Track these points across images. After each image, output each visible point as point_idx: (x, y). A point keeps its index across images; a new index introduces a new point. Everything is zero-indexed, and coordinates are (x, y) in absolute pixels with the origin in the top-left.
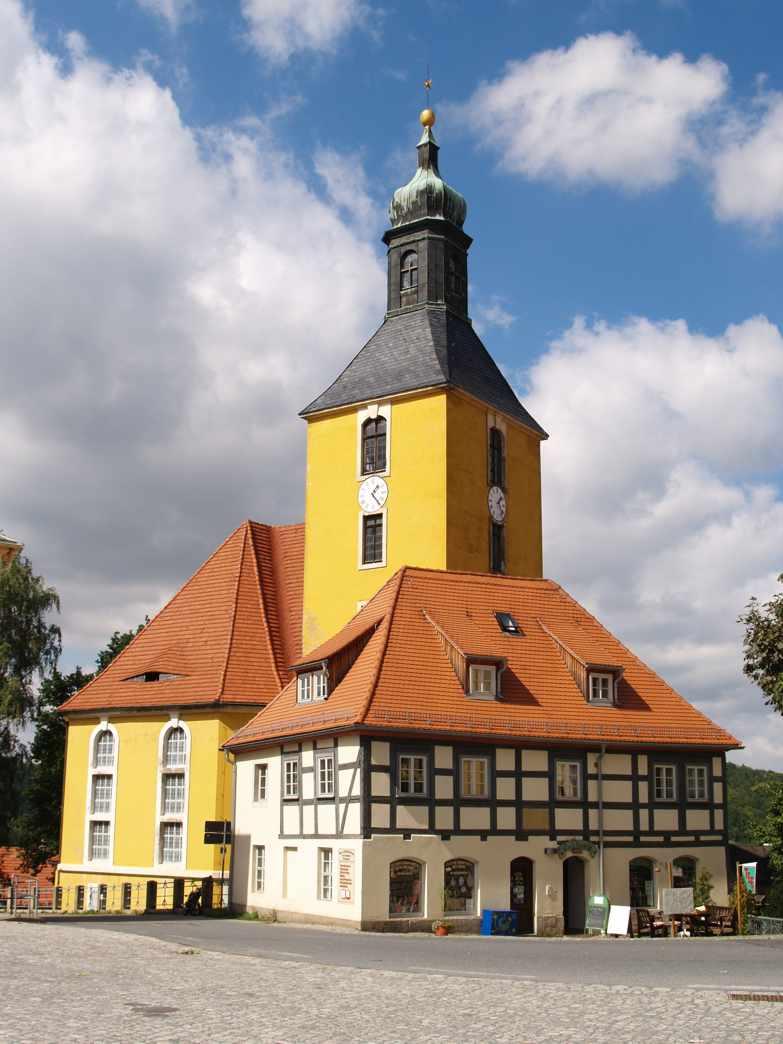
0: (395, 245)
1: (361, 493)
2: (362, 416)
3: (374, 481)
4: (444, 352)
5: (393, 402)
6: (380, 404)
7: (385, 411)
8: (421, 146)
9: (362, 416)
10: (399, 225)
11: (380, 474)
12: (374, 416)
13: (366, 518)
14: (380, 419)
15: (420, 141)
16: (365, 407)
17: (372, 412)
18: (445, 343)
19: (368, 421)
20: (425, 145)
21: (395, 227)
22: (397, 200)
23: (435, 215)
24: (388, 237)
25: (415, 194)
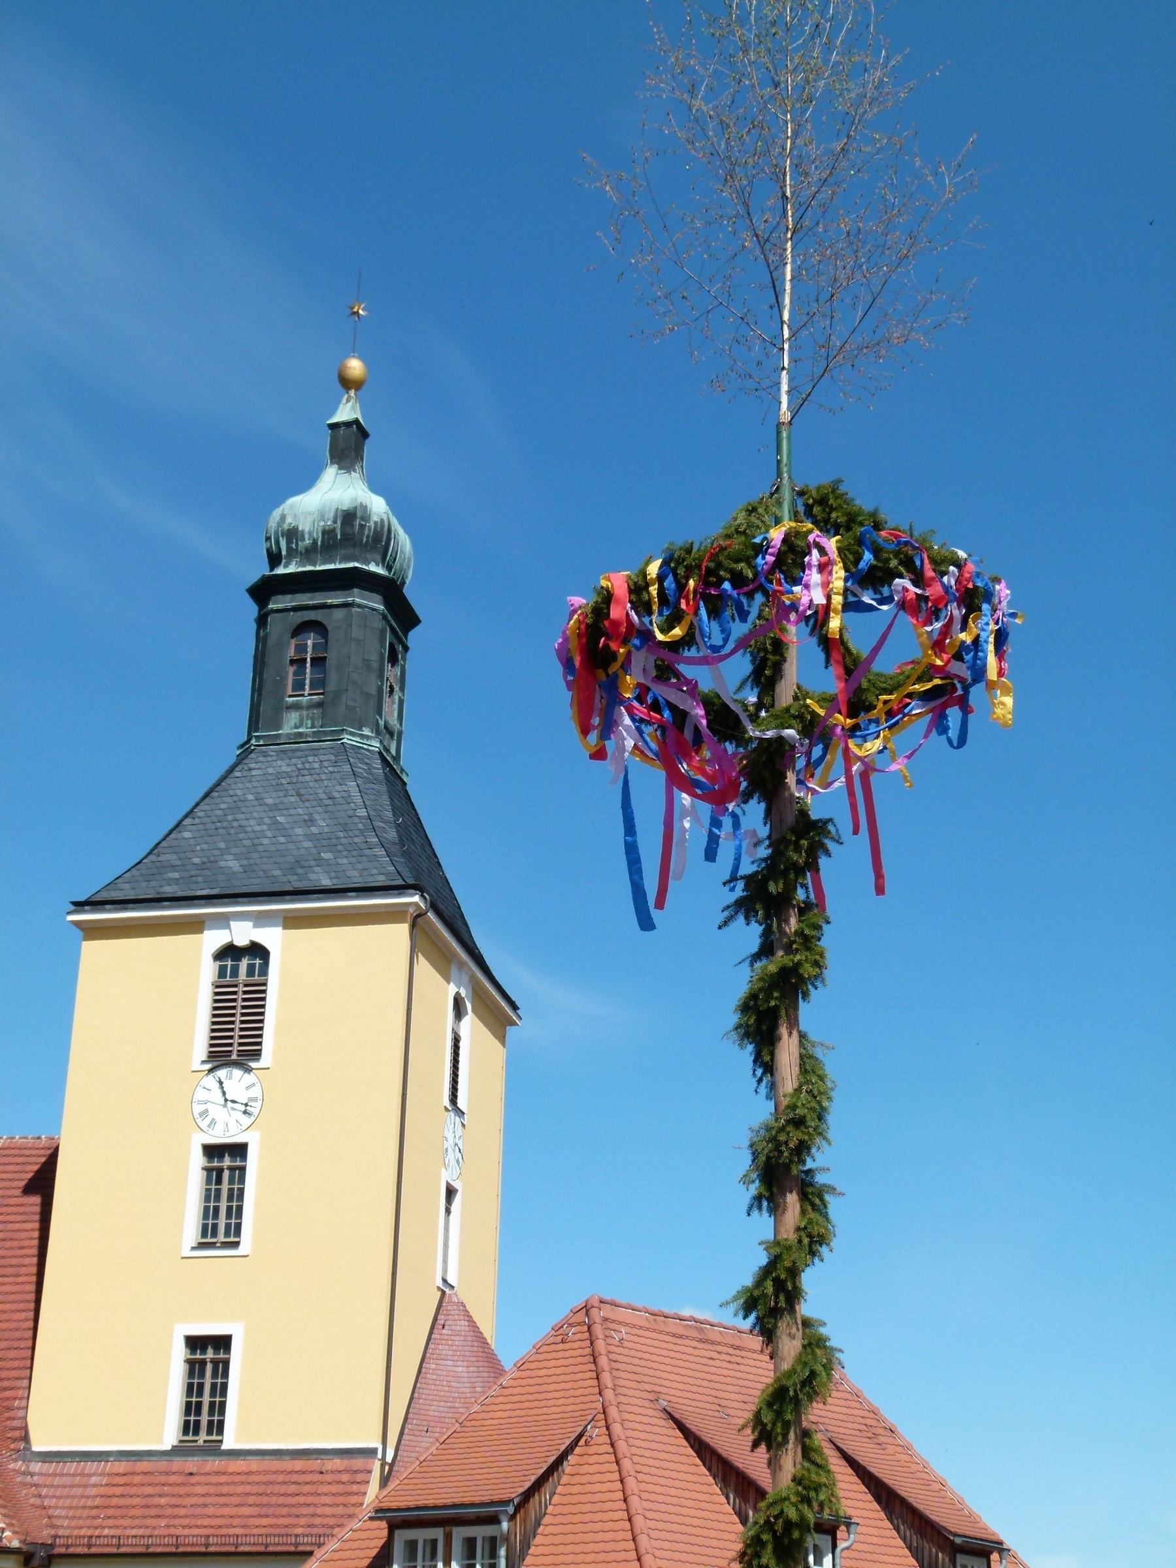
0: (280, 606)
1: (201, 1095)
2: (215, 939)
3: (236, 1081)
4: (392, 834)
5: (292, 921)
6: (261, 920)
7: (271, 937)
8: (333, 427)
9: (215, 939)
10: (292, 569)
11: (253, 1065)
12: (241, 941)
13: (211, 1151)
14: (258, 951)
15: (333, 412)
16: (223, 921)
17: (242, 933)
18: (389, 814)
19: (229, 952)
20: (348, 424)
21: (280, 571)
22: (289, 520)
23: (367, 563)
24: (262, 591)
25: (332, 515)
